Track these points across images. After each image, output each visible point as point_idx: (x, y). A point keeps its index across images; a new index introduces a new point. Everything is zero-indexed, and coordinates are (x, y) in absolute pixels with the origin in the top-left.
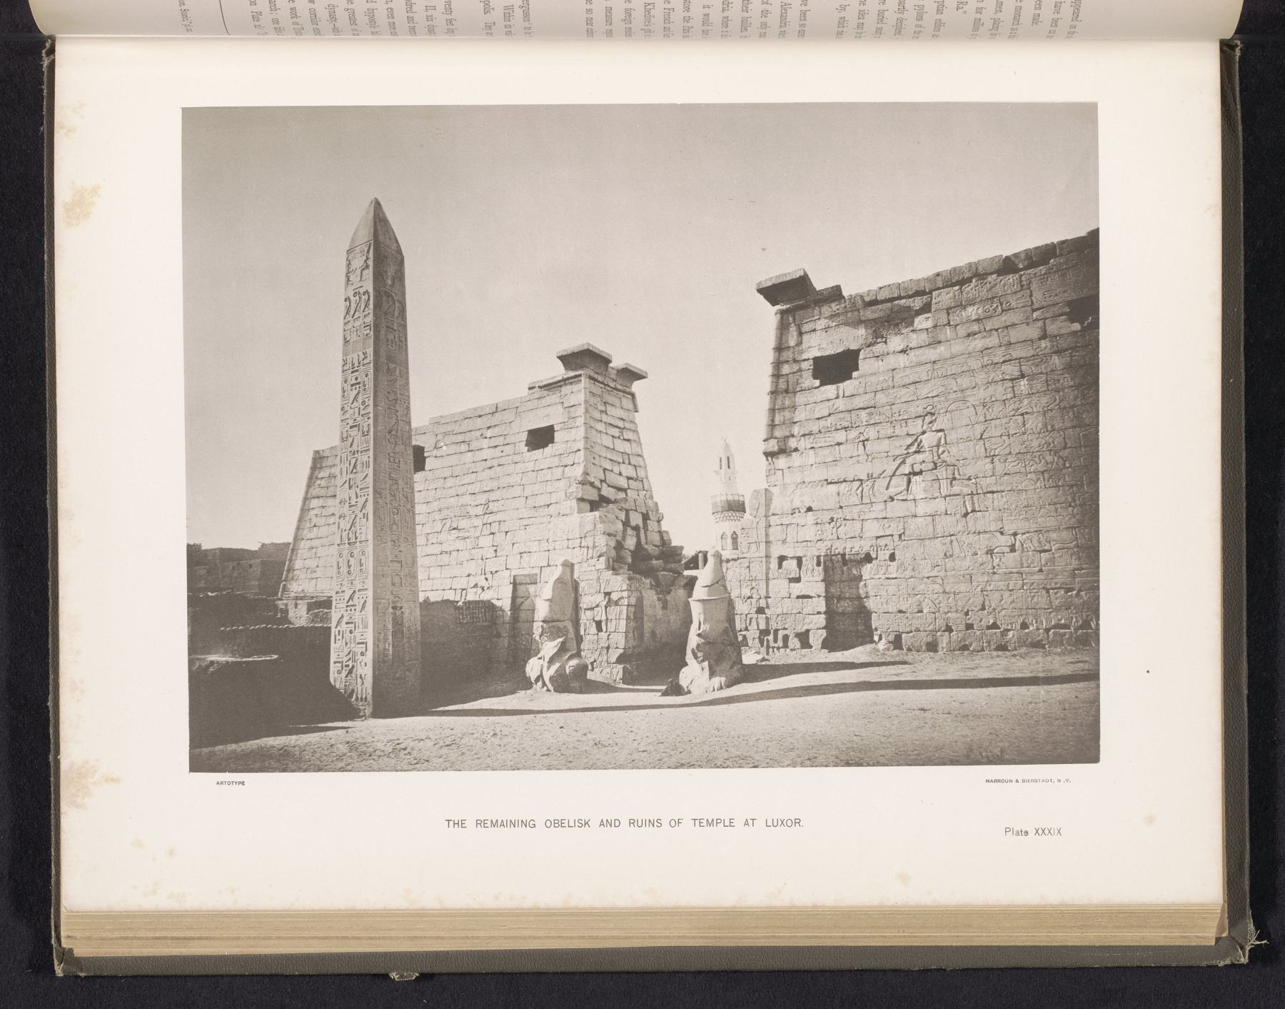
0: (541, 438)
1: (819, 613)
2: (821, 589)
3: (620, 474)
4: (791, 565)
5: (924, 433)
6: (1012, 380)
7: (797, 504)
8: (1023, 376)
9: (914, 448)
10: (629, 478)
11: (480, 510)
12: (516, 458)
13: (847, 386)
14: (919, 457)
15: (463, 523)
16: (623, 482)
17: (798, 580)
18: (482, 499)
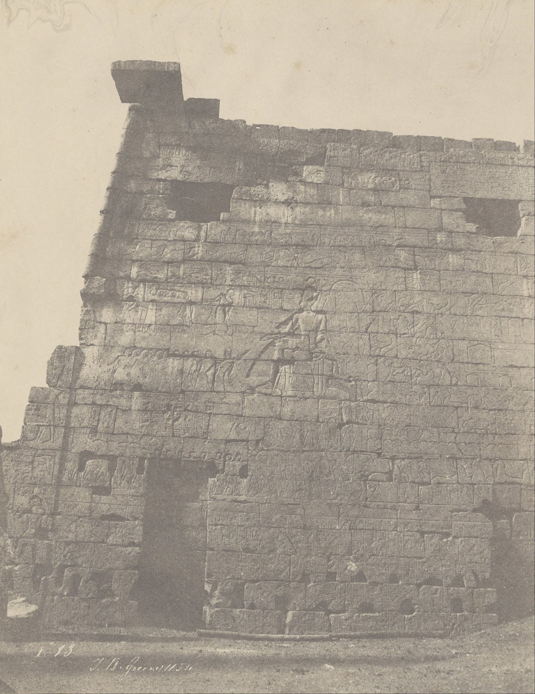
5: (301, 310)
6: (405, 269)
8: (416, 268)
9: (286, 329)
14: (292, 342)
17: (105, 490)
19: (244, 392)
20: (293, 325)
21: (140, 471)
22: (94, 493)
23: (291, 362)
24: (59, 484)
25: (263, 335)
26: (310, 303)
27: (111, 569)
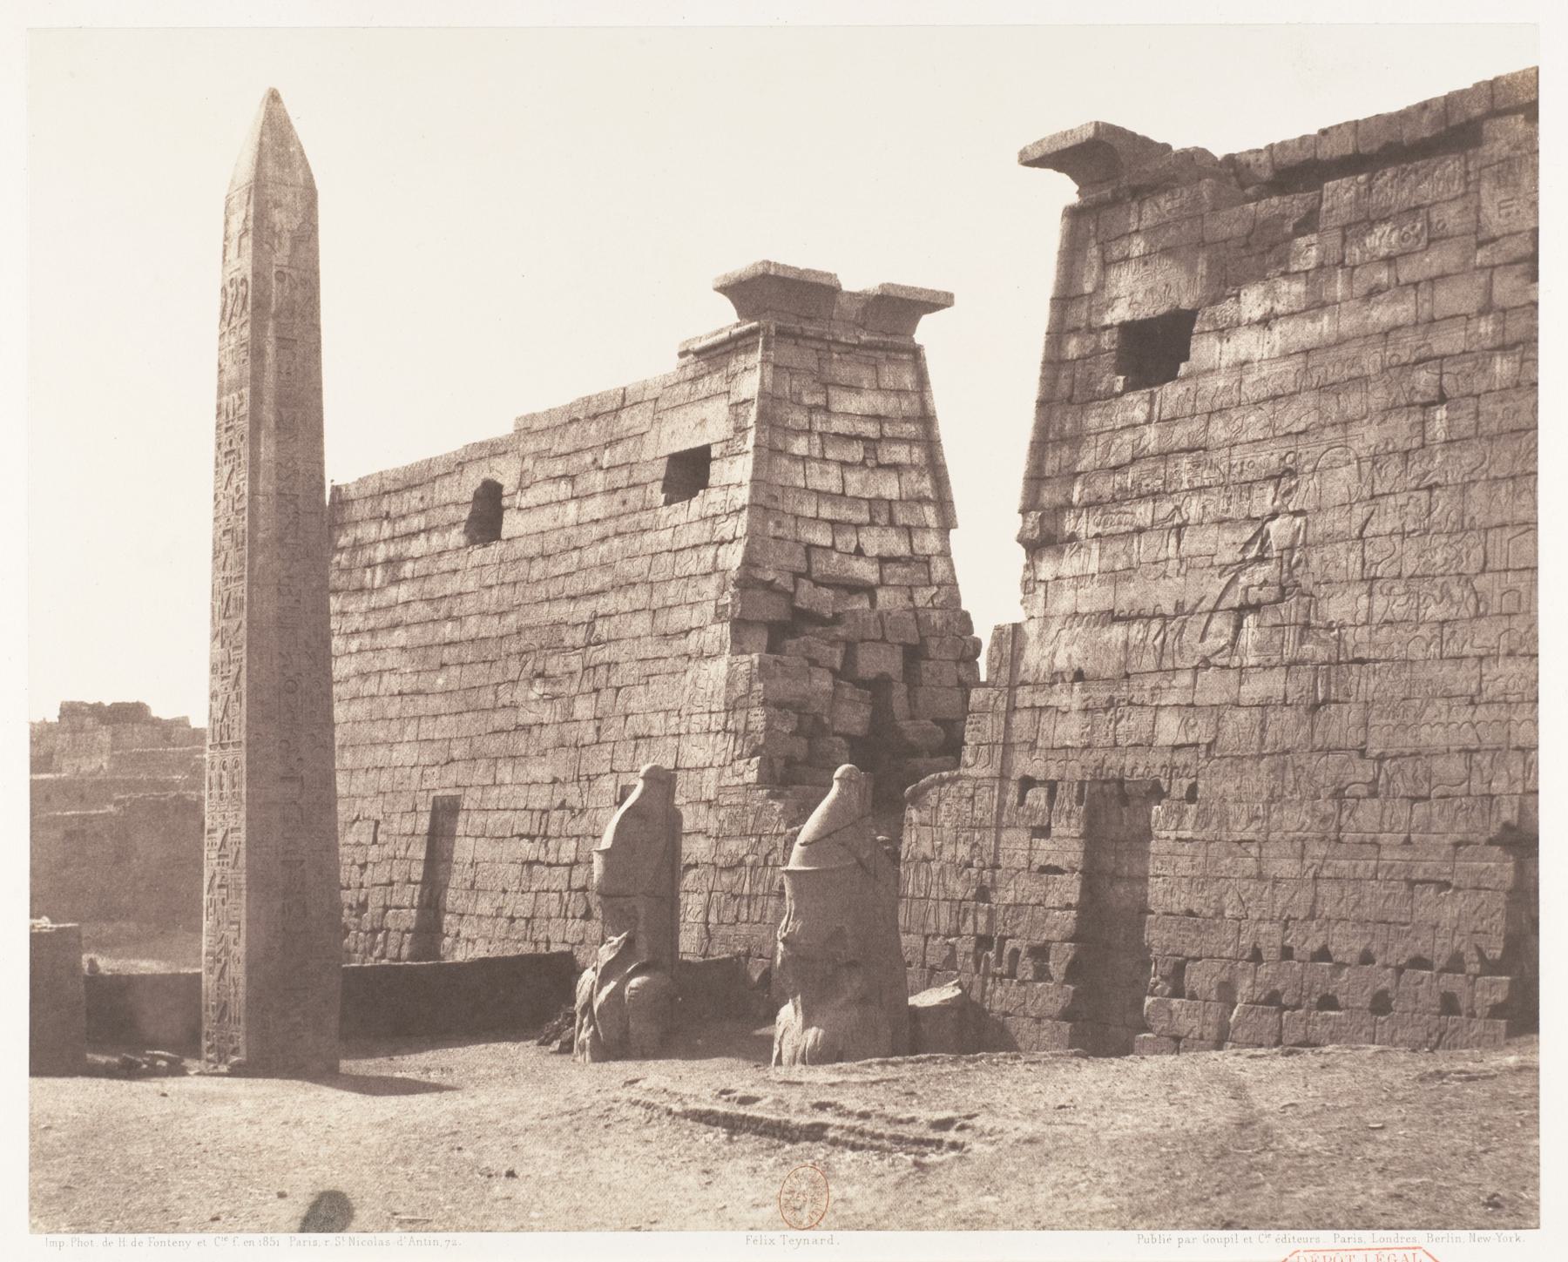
0: (689, 472)
1: (1069, 907)
2: (1073, 853)
3: (859, 552)
4: (1037, 797)
7: (1061, 663)
9: (1253, 552)
10: (883, 560)
11: (579, 636)
12: (646, 519)
13: (1172, 392)
15: (554, 665)
16: (865, 571)
17: (1044, 831)
18: (584, 610)
19: (1196, 668)
20: (1263, 543)
21: (1080, 801)
22: (1034, 835)
23: (1256, 608)
24: (999, 828)
25: (1225, 567)
26: (1286, 500)
27: (1047, 941)
